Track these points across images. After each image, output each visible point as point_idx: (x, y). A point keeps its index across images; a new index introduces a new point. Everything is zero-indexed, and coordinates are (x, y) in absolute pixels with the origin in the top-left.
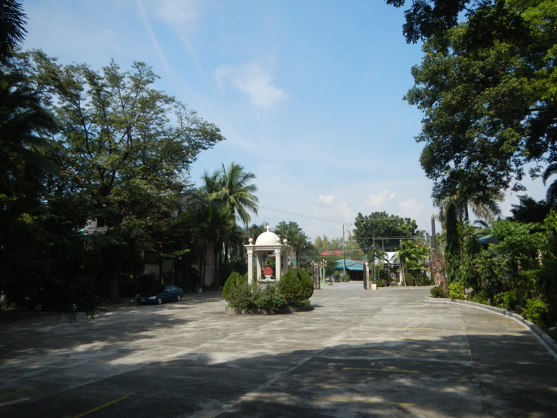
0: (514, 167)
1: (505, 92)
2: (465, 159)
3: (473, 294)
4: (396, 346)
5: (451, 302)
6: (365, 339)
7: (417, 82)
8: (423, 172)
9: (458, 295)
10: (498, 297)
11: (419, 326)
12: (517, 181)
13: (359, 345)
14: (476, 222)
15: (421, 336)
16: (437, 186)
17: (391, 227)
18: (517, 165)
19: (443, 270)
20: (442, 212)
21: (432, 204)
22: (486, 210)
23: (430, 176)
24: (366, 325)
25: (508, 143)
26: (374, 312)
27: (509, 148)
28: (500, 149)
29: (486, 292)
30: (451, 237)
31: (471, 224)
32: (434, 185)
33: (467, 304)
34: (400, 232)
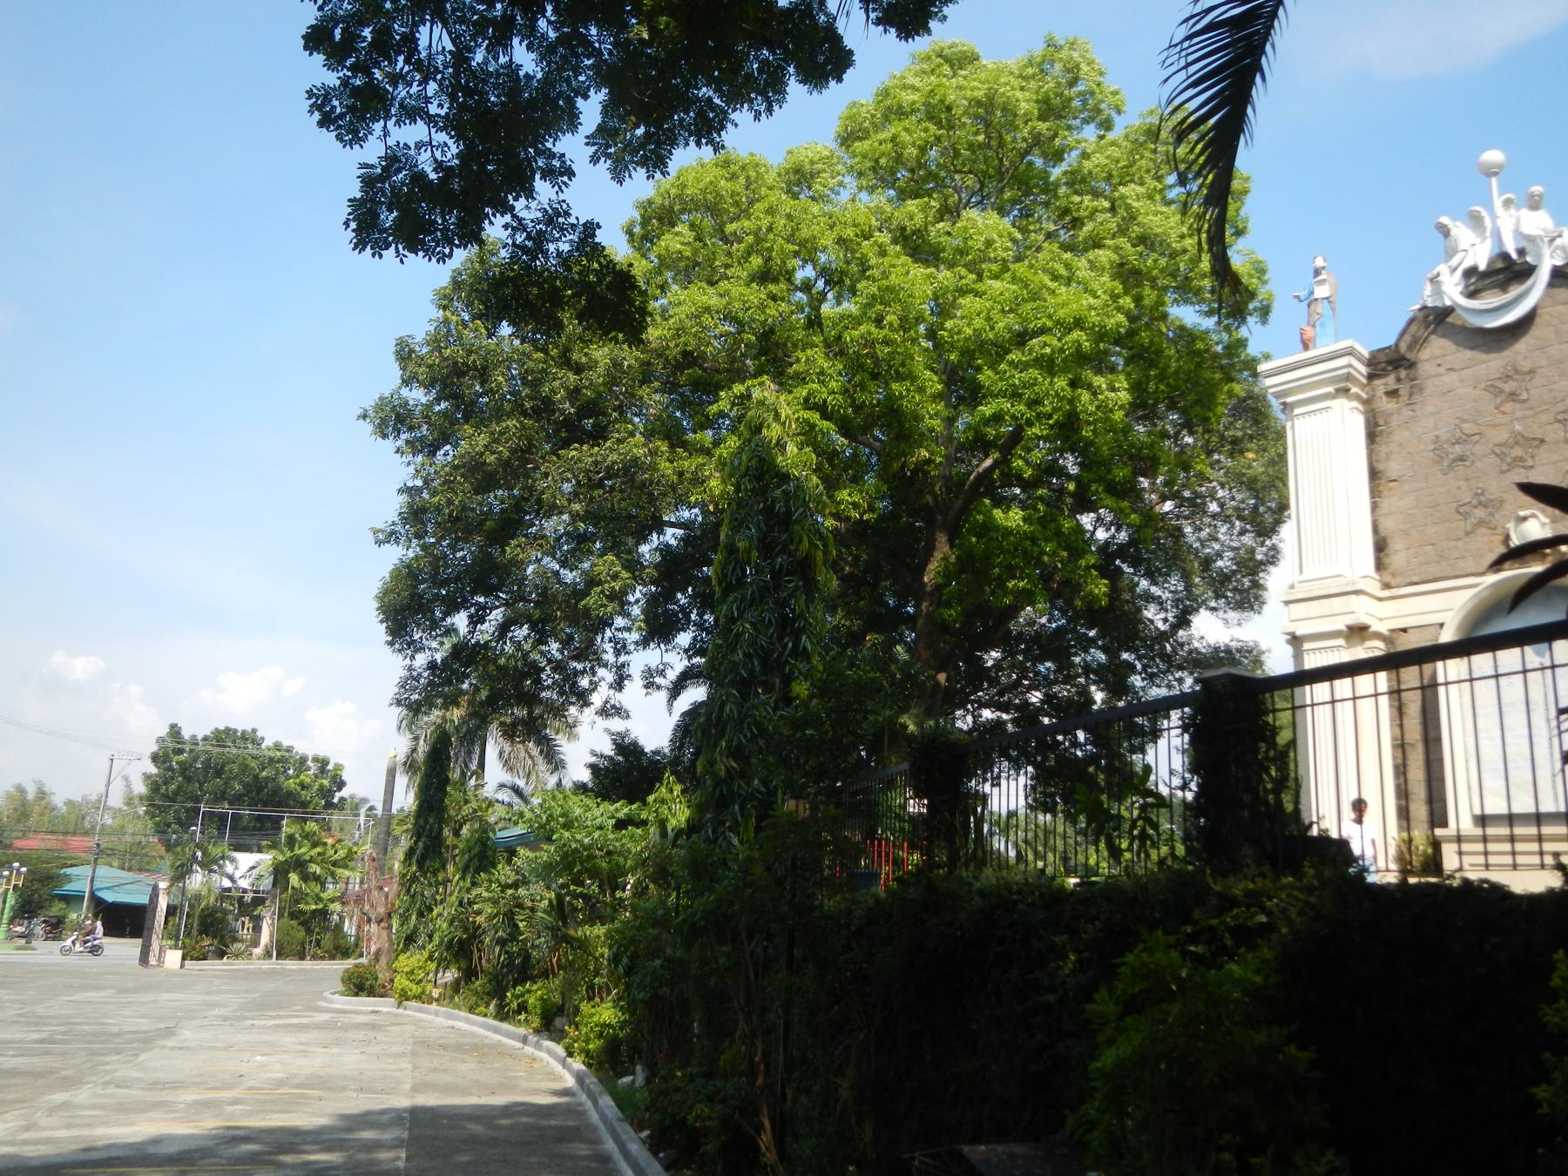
0: (609, 657)
1: (614, 463)
2: (497, 615)
3: (456, 987)
4: (181, 1153)
5: (394, 1010)
6: (86, 1132)
7: (406, 382)
9: (416, 989)
10: (517, 997)
11: (280, 1083)
12: (612, 692)
13: (58, 1155)
14: (502, 786)
15: (275, 1116)
16: (411, 677)
17: (267, 778)
18: (618, 653)
20: (414, 750)
21: (395, 722)
22: (531, 757)
23: (397, 646)
24: (106, 1084)
25: (602, 592)
26: (146, 1040)
27: (602, 606)
28: (583, 603)
29: (490, 981)
30: (426, 822)
31: (489, 791)
32: (404, 673)
33: (437, 1014)
34: (290, 794)
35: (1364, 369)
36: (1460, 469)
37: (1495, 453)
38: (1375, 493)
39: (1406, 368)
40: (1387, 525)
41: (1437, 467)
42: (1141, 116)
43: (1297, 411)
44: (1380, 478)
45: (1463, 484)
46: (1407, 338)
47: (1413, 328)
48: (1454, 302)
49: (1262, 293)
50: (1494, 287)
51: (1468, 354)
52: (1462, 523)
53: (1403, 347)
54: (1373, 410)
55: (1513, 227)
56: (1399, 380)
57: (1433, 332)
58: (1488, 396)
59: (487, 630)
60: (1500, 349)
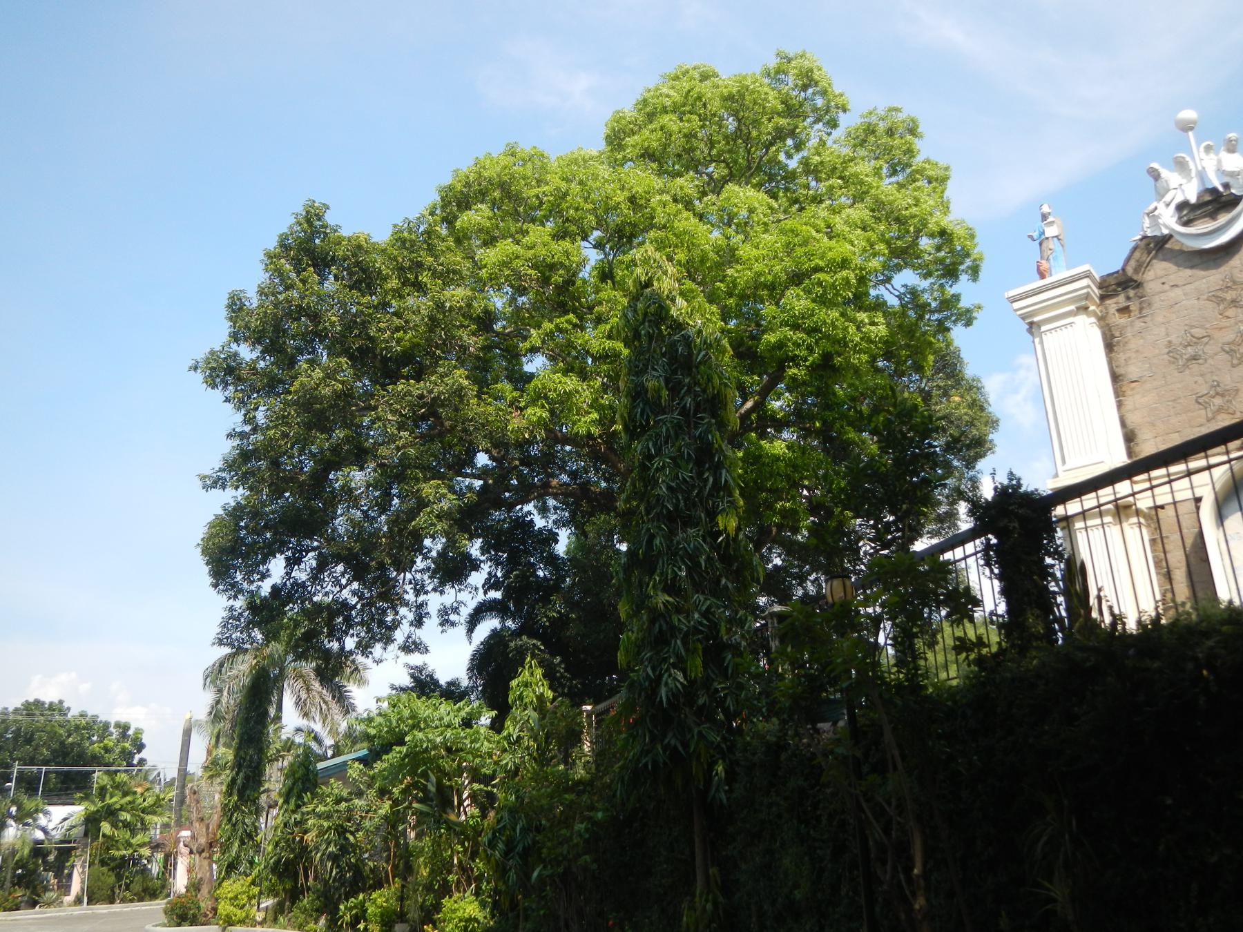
0: (410, 597)
1: (440, 393)
2: (310, 560)
3: (279, 910)
7: (235, 337)
8: (201, 571)
10: (351, 909)
12: (413, 629)
14: (299, 730)
18: (418, 592)
19: (211, 845)
20: (218, 702)
22: (325, 702)
23: (221, 587)
25: (432, 512)
27: (432, 524)
28: (413, 523)
29: (318, 898)
30: (246, 754)
31: (286, 734)
32: (225, 614)
35: (1096, 291)
36: (1194, 367)
37: (1224, 351)
38: (1119, 394)
39: (1134, 289)
40: (1132, 419)
41: (1173, 367)
42: (862, 116)
43: (1043, 328)
44: (1122, 380)
45: (1200, 380)
46: (1133, 263)
47: (1137, 254)
48: (1173, 230)
49: (975, 253)
50: (1205, 217)
51: (1188, 272)
52: (1203, 412)
53: (1130, 271)
54: (1108, 325)
55: (1214, 168)
56: (1128, 298)
57: (1155, 257)
58: (1210, 305)
59: (301, 574)
60: (1217, 266)
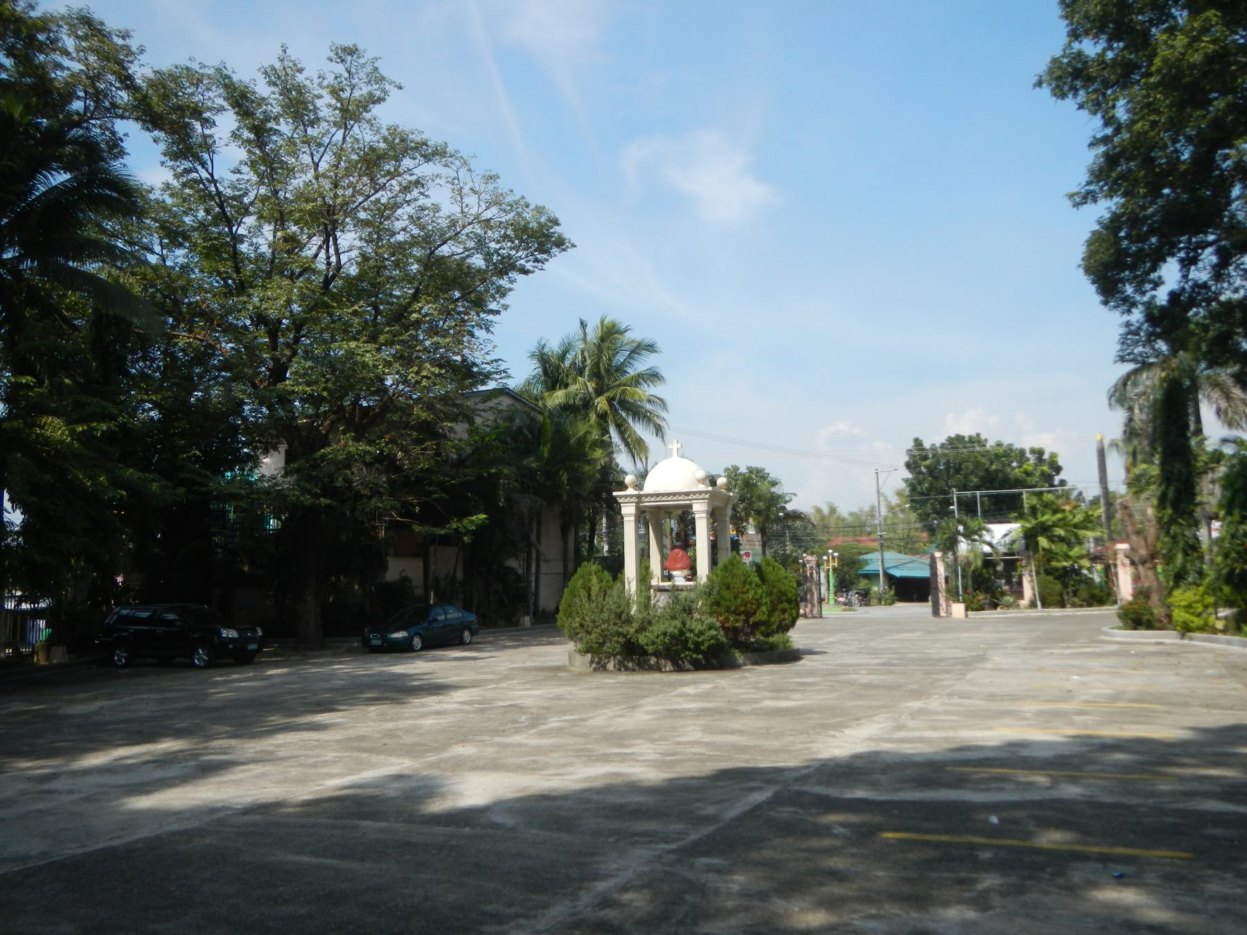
2: (1209, 257)
4: (1059, 757)
5: (1178, 641)
6: (951, 734)
7: (1075, 35)
8: (1088, 291)
9: (1197, 622)
11: (1115, 698)
13: (936, 753)
14: (1225, 441)
15: (1133, 727)
16: (1131, 332)
17: (997, 471)
19: (1153, 556)
20: (1130, 420)
21: (1106, 402)
24: (950, 695)
26: (968, 664)
31: (1210, 446)
32: (1123, 330)
33: (1229, 643)
59: (1201, 274)
